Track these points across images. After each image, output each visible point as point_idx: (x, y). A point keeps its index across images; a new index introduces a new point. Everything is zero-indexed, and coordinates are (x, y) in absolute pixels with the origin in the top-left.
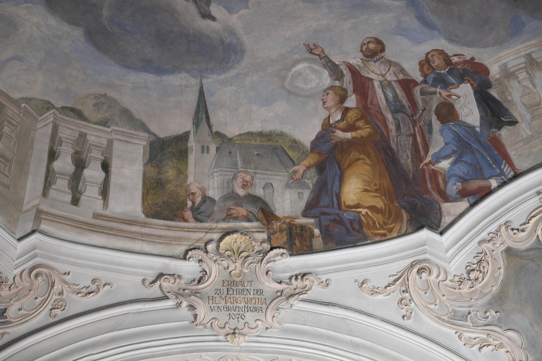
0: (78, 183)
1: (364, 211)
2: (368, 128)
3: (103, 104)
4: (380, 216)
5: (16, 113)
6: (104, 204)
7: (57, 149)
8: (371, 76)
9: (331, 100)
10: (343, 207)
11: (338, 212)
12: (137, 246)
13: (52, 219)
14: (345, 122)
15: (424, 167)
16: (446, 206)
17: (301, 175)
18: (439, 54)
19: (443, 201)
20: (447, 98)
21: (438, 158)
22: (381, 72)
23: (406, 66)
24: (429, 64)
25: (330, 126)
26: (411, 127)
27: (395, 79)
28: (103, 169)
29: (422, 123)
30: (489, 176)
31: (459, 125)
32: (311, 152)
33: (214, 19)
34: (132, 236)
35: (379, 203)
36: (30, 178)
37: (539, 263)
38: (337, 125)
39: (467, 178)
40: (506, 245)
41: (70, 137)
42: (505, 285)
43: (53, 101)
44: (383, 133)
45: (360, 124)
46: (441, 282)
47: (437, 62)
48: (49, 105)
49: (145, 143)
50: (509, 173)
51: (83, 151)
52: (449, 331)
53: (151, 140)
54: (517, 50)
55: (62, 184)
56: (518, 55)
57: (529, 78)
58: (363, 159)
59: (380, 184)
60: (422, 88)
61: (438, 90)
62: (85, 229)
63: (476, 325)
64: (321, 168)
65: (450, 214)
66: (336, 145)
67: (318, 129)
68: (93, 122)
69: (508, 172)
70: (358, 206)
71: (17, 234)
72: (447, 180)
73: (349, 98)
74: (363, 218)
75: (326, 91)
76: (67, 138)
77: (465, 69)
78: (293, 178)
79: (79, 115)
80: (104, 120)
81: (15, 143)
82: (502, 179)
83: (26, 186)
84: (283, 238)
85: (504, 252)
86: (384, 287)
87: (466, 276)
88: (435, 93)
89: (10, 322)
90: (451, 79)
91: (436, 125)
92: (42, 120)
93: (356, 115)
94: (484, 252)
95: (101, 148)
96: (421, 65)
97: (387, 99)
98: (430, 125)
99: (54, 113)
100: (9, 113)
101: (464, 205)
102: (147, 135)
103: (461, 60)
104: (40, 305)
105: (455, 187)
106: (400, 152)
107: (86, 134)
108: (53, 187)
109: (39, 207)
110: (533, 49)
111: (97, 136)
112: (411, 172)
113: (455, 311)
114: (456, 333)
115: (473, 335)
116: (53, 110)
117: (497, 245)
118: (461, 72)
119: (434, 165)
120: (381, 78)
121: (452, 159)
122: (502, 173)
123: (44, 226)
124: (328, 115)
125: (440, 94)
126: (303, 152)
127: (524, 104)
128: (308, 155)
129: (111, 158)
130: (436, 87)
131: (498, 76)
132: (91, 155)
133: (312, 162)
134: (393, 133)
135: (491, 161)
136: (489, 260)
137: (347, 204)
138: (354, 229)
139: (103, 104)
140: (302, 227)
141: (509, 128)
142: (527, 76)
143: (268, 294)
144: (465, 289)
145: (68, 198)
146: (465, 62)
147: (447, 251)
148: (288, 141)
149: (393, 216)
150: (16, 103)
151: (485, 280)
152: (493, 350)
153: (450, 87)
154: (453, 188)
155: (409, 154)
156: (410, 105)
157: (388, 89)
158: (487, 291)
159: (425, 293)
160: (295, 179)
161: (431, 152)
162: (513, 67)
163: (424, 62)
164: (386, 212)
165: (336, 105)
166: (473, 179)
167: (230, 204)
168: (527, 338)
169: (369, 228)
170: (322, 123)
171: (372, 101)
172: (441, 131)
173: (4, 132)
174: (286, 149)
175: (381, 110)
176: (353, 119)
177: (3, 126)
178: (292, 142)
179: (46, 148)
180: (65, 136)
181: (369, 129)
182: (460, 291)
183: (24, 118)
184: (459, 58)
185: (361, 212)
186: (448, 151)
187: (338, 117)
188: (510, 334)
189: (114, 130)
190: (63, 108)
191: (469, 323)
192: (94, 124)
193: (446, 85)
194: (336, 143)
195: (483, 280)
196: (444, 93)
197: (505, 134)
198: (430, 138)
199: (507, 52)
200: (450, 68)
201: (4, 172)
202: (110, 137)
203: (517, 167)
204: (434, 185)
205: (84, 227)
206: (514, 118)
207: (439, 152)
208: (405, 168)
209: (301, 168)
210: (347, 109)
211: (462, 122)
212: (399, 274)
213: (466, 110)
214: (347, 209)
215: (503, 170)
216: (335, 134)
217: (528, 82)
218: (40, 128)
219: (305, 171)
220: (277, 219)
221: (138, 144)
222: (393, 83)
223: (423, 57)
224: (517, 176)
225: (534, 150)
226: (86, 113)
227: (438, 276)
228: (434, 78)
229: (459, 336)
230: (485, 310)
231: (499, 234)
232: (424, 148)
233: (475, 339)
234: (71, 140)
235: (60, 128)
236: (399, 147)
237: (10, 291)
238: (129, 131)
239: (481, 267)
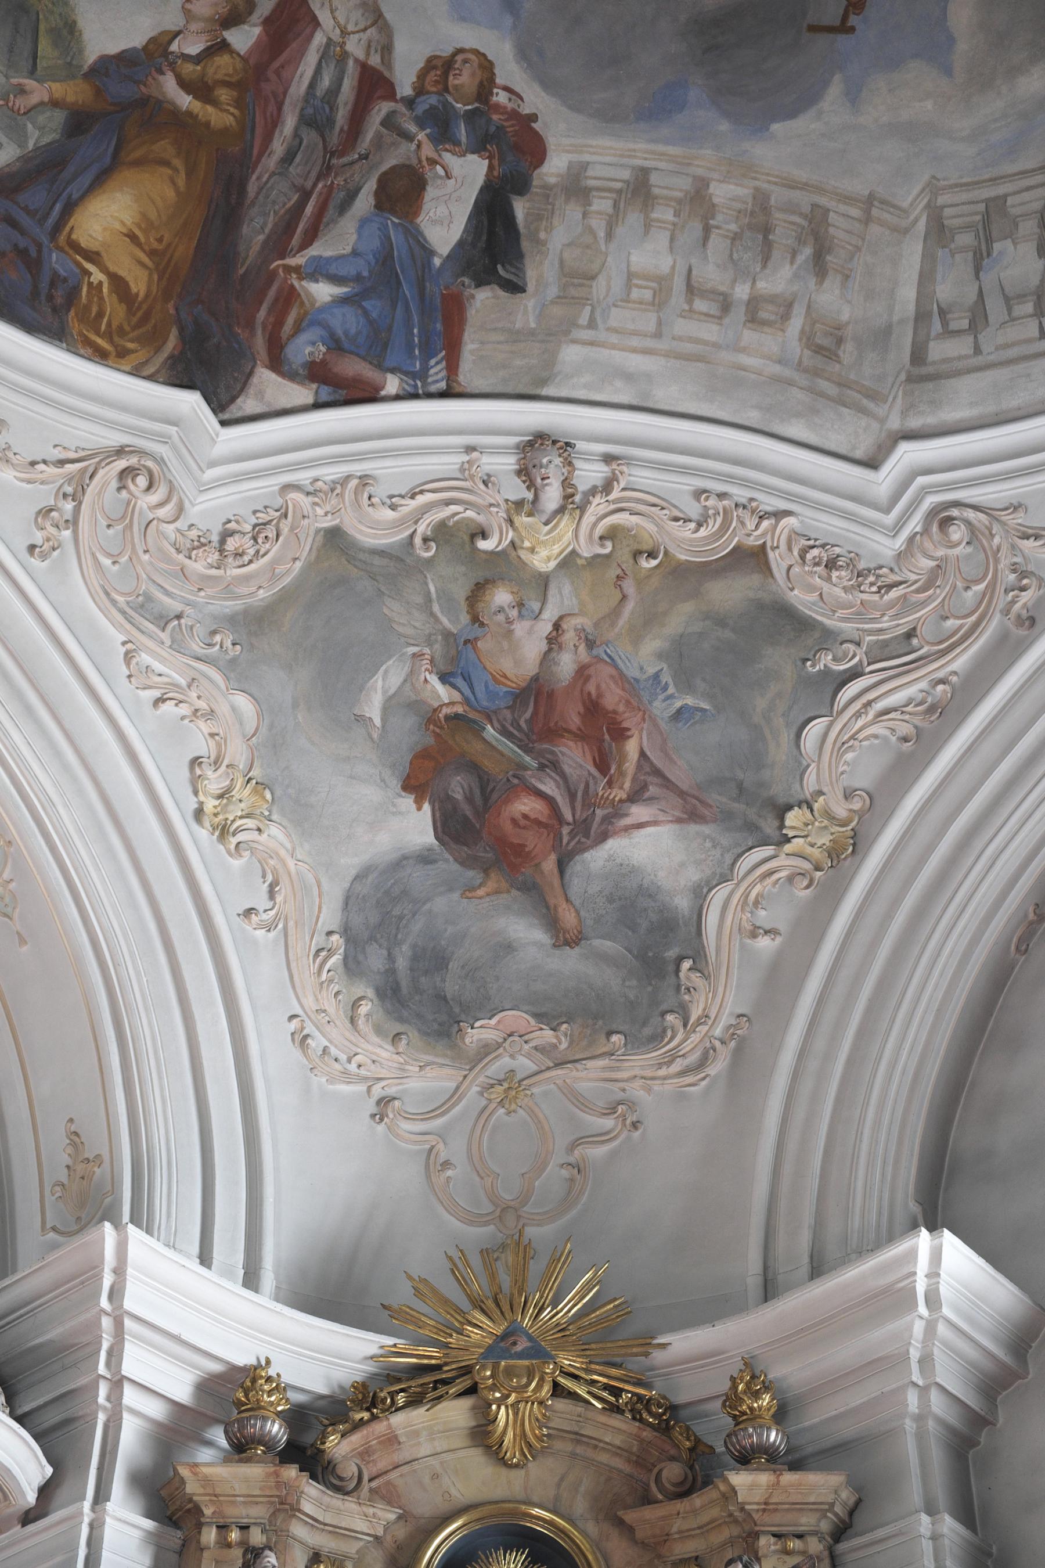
1: (97, 276)
2: (232, 114)
4: (121, 310)
8: (324, 17)
10: (62, 238)
11: (45, 240)
14: (199, 68)
15: (281, 271)
16: (265, 377)
17: (29, 107)
18: (481, 66)
19: (267, 363)
20: (425, 163)
21: (319, 271)
22: (348, 21)
23: (401, 46)
24: (445, 74)
25: (166, 53)
26: (314, 175)
27: (361, 56)
29: (340, 181)
30: (393, 364)
31: (407, 232)
32: (86, 76)
35: (139, 283)
37: (383, 589)
38: (180, 62)
39: (346, 345)
40: (337, 521)
42: (285, 598)
44: (252, 146)
45: (224, 95)
46: (155, 522)
47: (465, 79)
50: (437, 381)
52: (112, 630)
54: (629, 150)
56: (625, 161)
57: (611, 216)
58: (176, 170)
59: (169, 245)
60: (394, 112)
61: (421, 136)
63: (177, 646)
65: (263, 397)
66: (144, 102)
67: (137, 40)
69: (435, 378)
70: (92, 257)
72: (304, 324)
73: (246, 27)
74: (85, 289)
77: (503, 127)
78: (7, 101)
82: (416, 386)
85: (322, 533)
86: (30, 460)
87: (215, 538)
88: (409, 137)
90: (462, 132)
91: (365, 202)
93: (231, 71)
94: (283, 511)
96: (431, 64)
97: (312, 85)
98: (352, 196)
101: (303, 394)
103: (510, 106)
105: (308, 349)
106: (255, 210)
110: (662, 165)
112: (248, 262)
113: (149, 598)
114: (124, 643)
115: (158, 667)
117: (320, 511)
118: (492, 129)
119: (300, 278)
120: (336, 35)
121: (345, 290)
122: (423, 375)
124: (177, 29)
125: (419, 146)
126: (70, 64)
127: (562, 262)
128: (74, 77)
130: (422, 128)
131: (552, 180)
133: (71, 98)
134: (271, 162)
135: (416, 339)
136: (285, 530)
137: (74, 236)
138: (50, 298)
141: (501, 293)
142: (610, 211)
144: (200, 565)
146: (514, 115)
147: (212, 464)
148: (60, 14)
149: (149, 327)
151: (253, 566)
152: (183, 718)
153: (447, 146)
155: (270, 226)
156: (346, 128)
157: (332, 66)
158: (244, 590)
159: (109, 526)
160: (10, 104)
161: (314, 251)
162: (595, 178)
163: (440, 64)
164: (139, 308)
165: (210, 20)
166: (358, 355)
168: (271, 727)
169: (83, 318)
170: (152, 34)
171: (283, 67)
172: (363, 222)
174: (42, 27)
175: (285, 96)
176: (219, 76)
178: (66, 23)
181: (231, 118)
182: (187, 561)
184: (510, 100)
185: (90, 274)
186: (348, 269)
187: (194, 49)
188: (242, 701)
191: (165, 636)
193: (443, 136)
194: (150, 97)
195: (251, 562)
196: (428, 150)
198: (334, 221)
199: (606, 142)
200: (477, 109)
203: (461, 378)
204: (272, 319)
206: (524, 278)
207: (329, 260)
208: (242, 248)
209: (38, 92)
210: (223, 46)
211: (417, 229)
212: (82, 454)
213: (442, 211)
214: (67, 249)
215: (428, 370)
216: (161, 78)
217: (603, 223)
219: (42, 103)
222: (351, 63)
223: (446, 51)
225: (518, 362)
227: (161, 505)
228: (432, 108)
229: (127, 653)
230: (214, 627)
231: (338, 491)
232: (306, 232)
233: (160, 675)
236: (261, 198)
239: (263, 535)
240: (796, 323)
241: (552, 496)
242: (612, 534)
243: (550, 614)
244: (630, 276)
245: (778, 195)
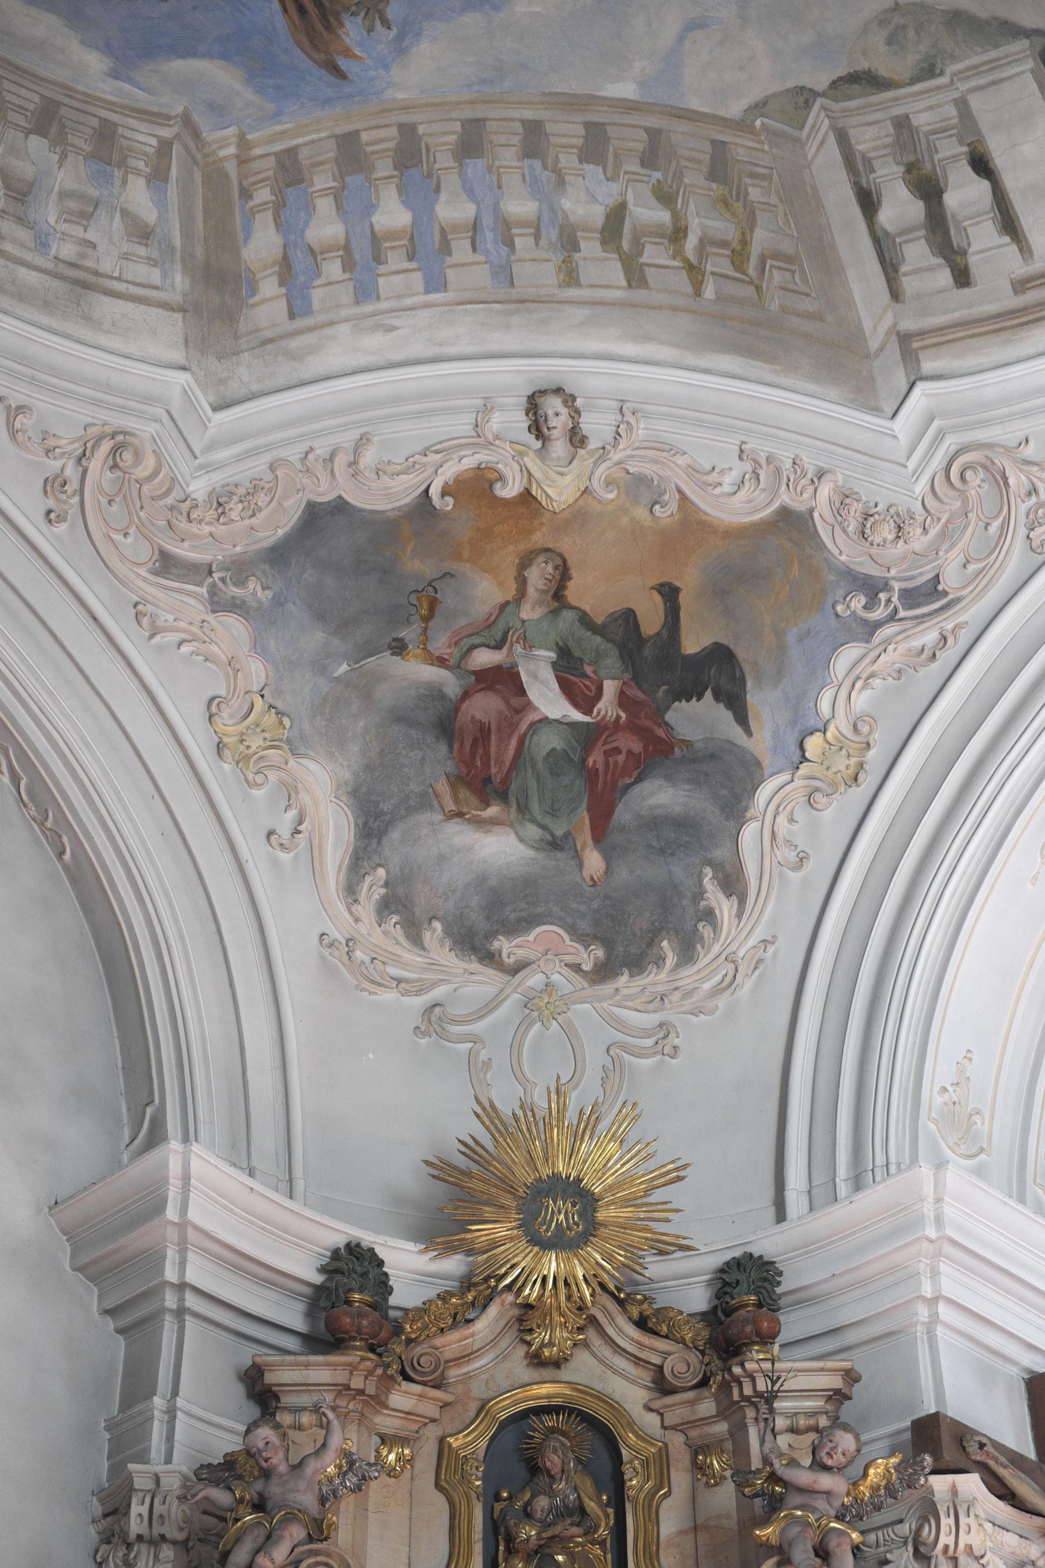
0: (946, 233)
3: (904, 27)
5: (755, 149)
6: (1021, 250)
7: (868, 182)
13: (935, 340)
28: (978, 174)
36: (851, 274)
41: (879, 143)
43: (807, 82)
48: (806, 94)
49: (1030, 64)
51: (920, 158)
53: (1038, 49)
62: (1012, 327)
68: (907, 81)
71: (885, 409)
76: (876, 149)
80: (925, 65)
81: (786, 215)
83: (853, 297)
89: (958, 600)
92: (809, 135)
95: (952, 128)
99: (823, 108)
100: (742, 154)
102: (1026, 43)
104: (1000, 536)
107: (907, 117)
108: (904, 269)
109: (898, 328)
111: (931, 108)
116: (819, 101)
129: (981, 140)
132: (940, 156)
139: (904, 27)
145: (945, 277)
150: (743, 125)
173: (753, 202)
177: (746, 189)
179: (848, 193)
180: (870, 145)
183: (774, 150)
189: (955, 74)
190: (834, 85)
192: (909, 84)
201: (796, 288)
202: (956, 95)
205: (1008, 324)
218: (815, 156)
221: (1018, 74)
226: (884, 71)
234: (885, 147)
235: (852, 133)
237: (927, 534)
238: (985, 57)
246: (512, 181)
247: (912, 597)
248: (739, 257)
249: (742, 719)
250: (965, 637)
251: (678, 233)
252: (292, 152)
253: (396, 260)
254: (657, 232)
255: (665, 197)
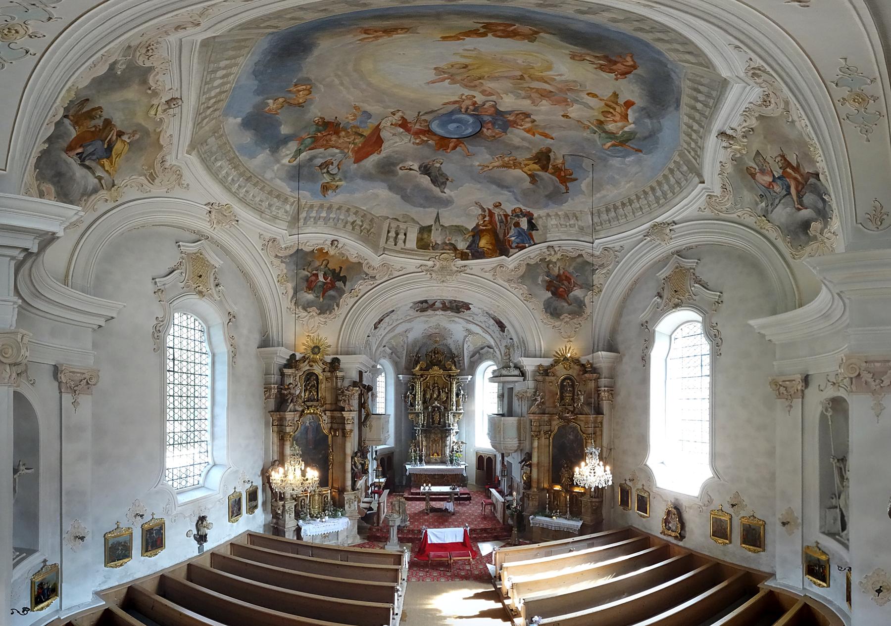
9: (480, 217)
12: (415, 257)
16: (511, 250)
21: (511, 237)
33: (445, 193)
34: (413, 255)
55: (392, 240)
64: (473, 236)
75: (479, 215)
79: (397, 220)
84: (460, 255)
91: (513, 227)
101: (517, 250)
123: (386, 252)
140: (465, 252)
143: (454, 271)
144: (513, 273)
145: (394, 244)
150: (378, 217)
154: (514, 245)
167: (444, 245)
186: (516, 234)
197: (534, 232)
209: (467, 236)
220: (458, 250)
224: (535, 244)
240: (577, 227)
241: (553, 253)
242: (562, 255)
243: (558, 266)
244: (552, 225)
245: (568, 212)
246: (342, 214)
247: (371, 277)
248: (368, 231)
249: (345, 286)
250: (376, 284)
251: (362, 226)
252: (313, 205)
253: (321, 220)
254: (359, 225)
255: (362, 221)
